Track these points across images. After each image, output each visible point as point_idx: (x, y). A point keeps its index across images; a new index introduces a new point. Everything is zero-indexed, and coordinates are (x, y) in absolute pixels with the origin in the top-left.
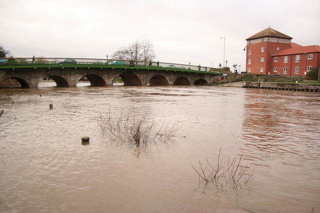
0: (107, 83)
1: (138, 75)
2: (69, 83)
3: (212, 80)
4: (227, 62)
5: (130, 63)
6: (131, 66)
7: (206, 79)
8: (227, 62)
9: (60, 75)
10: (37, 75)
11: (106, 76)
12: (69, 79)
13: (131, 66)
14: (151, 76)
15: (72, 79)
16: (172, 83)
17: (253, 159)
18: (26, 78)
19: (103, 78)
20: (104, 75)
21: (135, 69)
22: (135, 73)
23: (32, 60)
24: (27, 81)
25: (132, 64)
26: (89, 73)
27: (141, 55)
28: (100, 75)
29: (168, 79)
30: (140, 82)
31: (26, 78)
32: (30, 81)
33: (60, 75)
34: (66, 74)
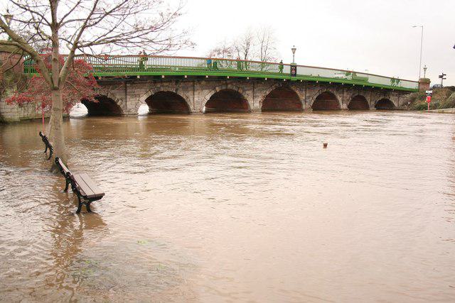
0: (252, 107)
1: (297, 92)
2: (191, 107)
3: (401, 101)
4: (425, 69)
5: (292, 70)
6: (292, 75)
7: (393, 99)
8: (425, 69)
9: (177, 90)
10: (137, 91)
11: (250, 92)
12: (191, 99)
13: (292, 75)
14: (315, 93)
15: (196, 99)
16: (344, 106)
17: (269, 171)
18: (118, 97)
19: (246, 96)
20: (247, 92)
21: (298, 81)
22: (293, 88)
23: (234, 67)
24: (118, 104)
25: (294, 71)
26: (224, 88)
27: (254, 55)
28: (240, 91)
29: (340, 99)
30: (300, 104)
31: (118, 97)
32: (124, 103)
33: (177, 90)
34: (186, 89)
